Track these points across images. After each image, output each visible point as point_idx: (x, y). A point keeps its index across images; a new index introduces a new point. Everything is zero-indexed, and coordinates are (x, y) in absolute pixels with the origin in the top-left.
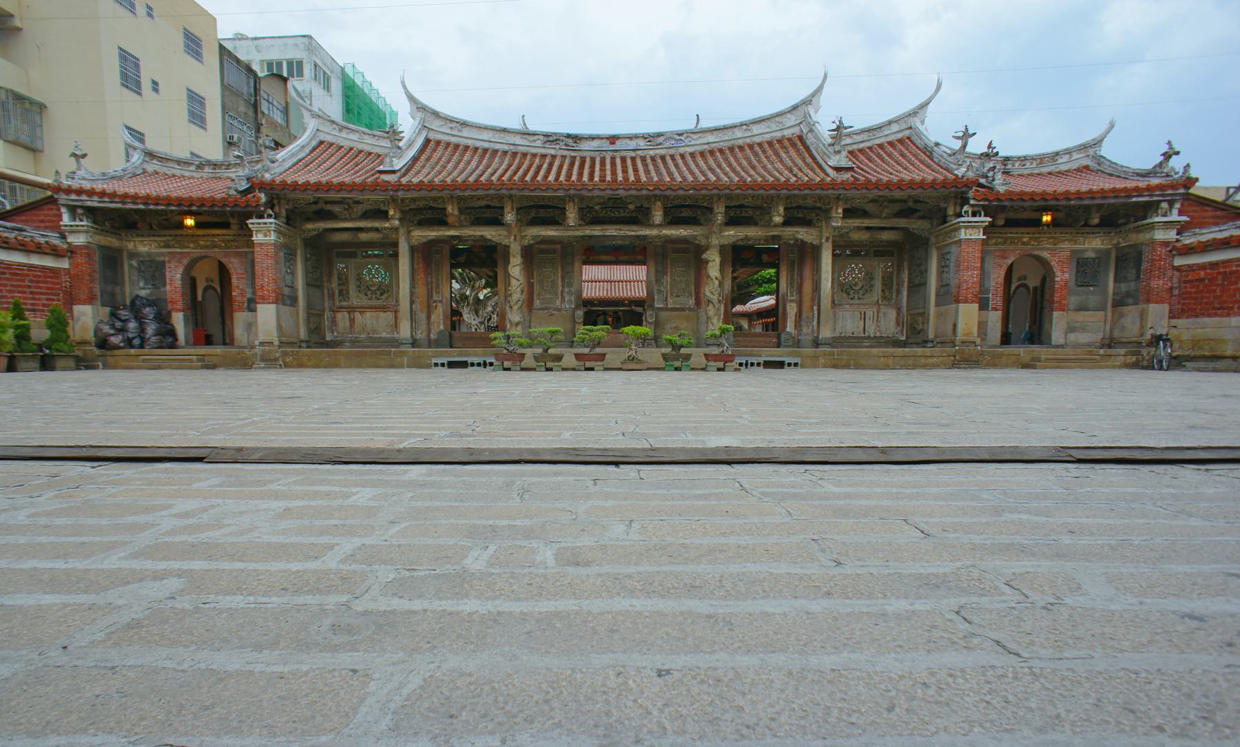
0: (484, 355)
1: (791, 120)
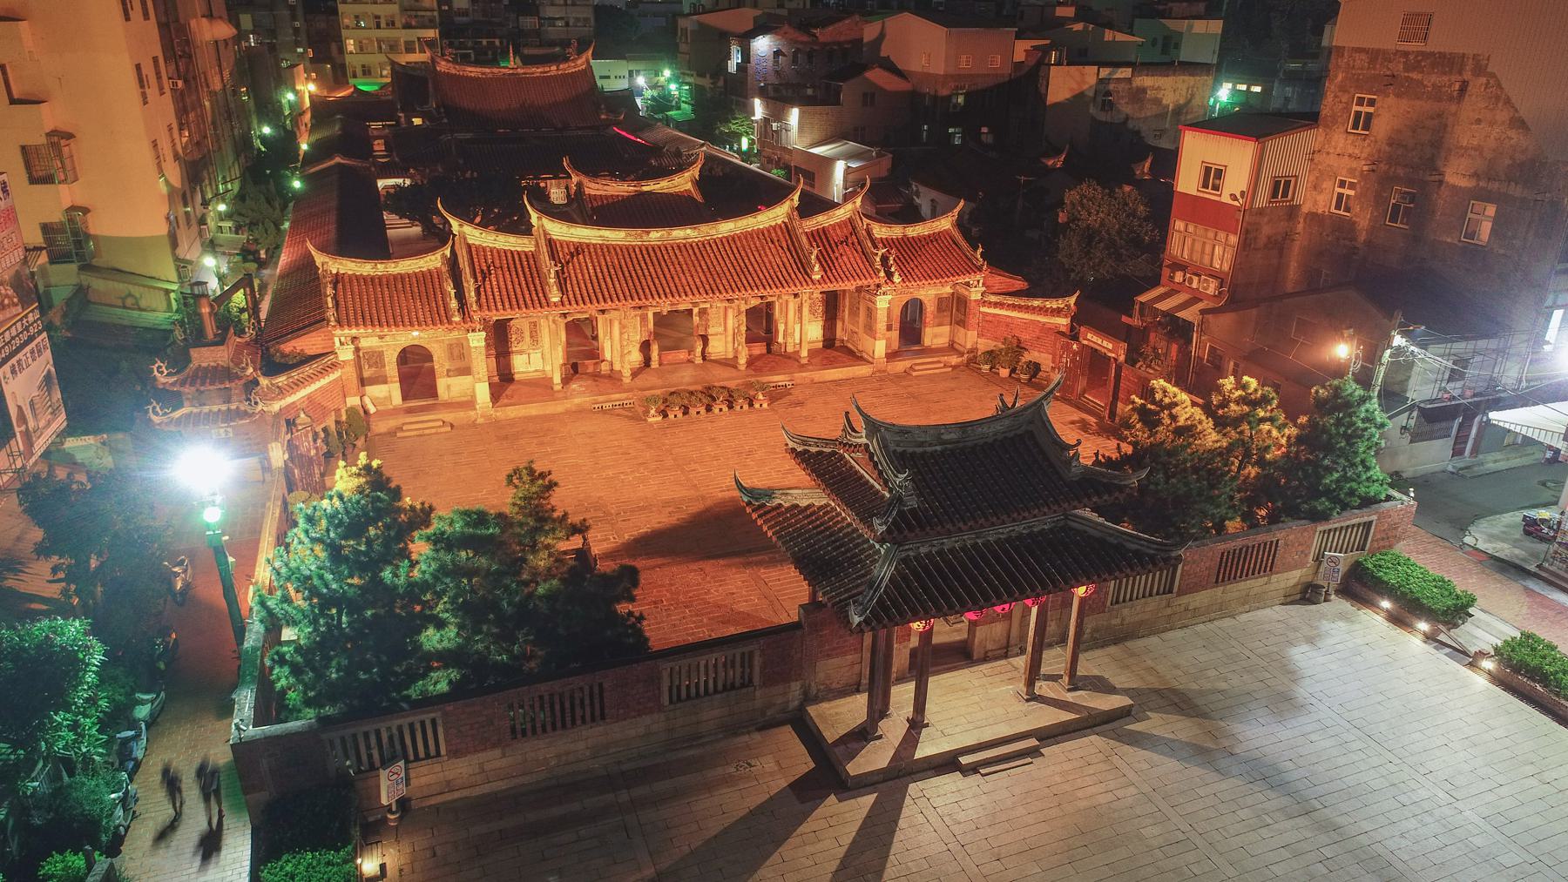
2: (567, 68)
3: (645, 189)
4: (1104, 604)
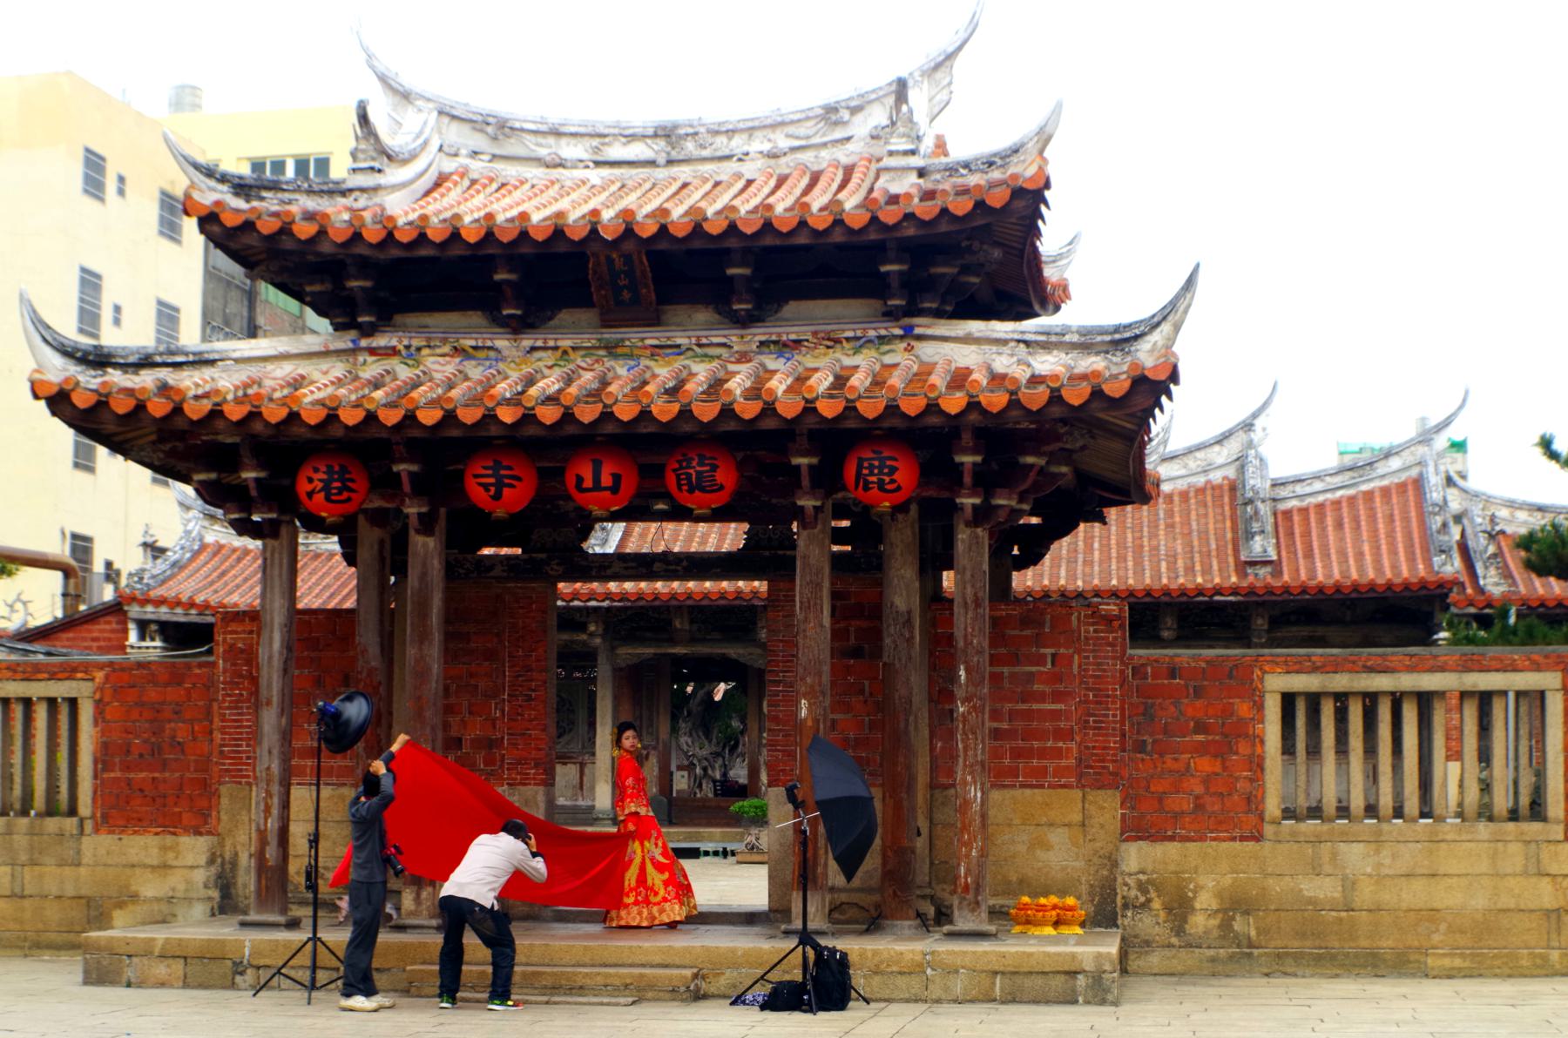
0: (724, 838)
1: (1221, 455)
4: (1253, 802)
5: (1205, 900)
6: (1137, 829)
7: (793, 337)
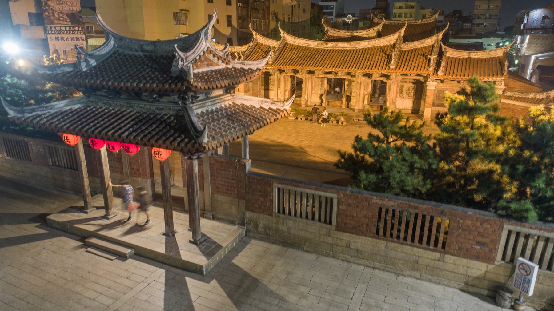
2: (479, 41)
3: (355, 34)
5: (261, 225)
6: (248, 209)
7: (161, 107)
